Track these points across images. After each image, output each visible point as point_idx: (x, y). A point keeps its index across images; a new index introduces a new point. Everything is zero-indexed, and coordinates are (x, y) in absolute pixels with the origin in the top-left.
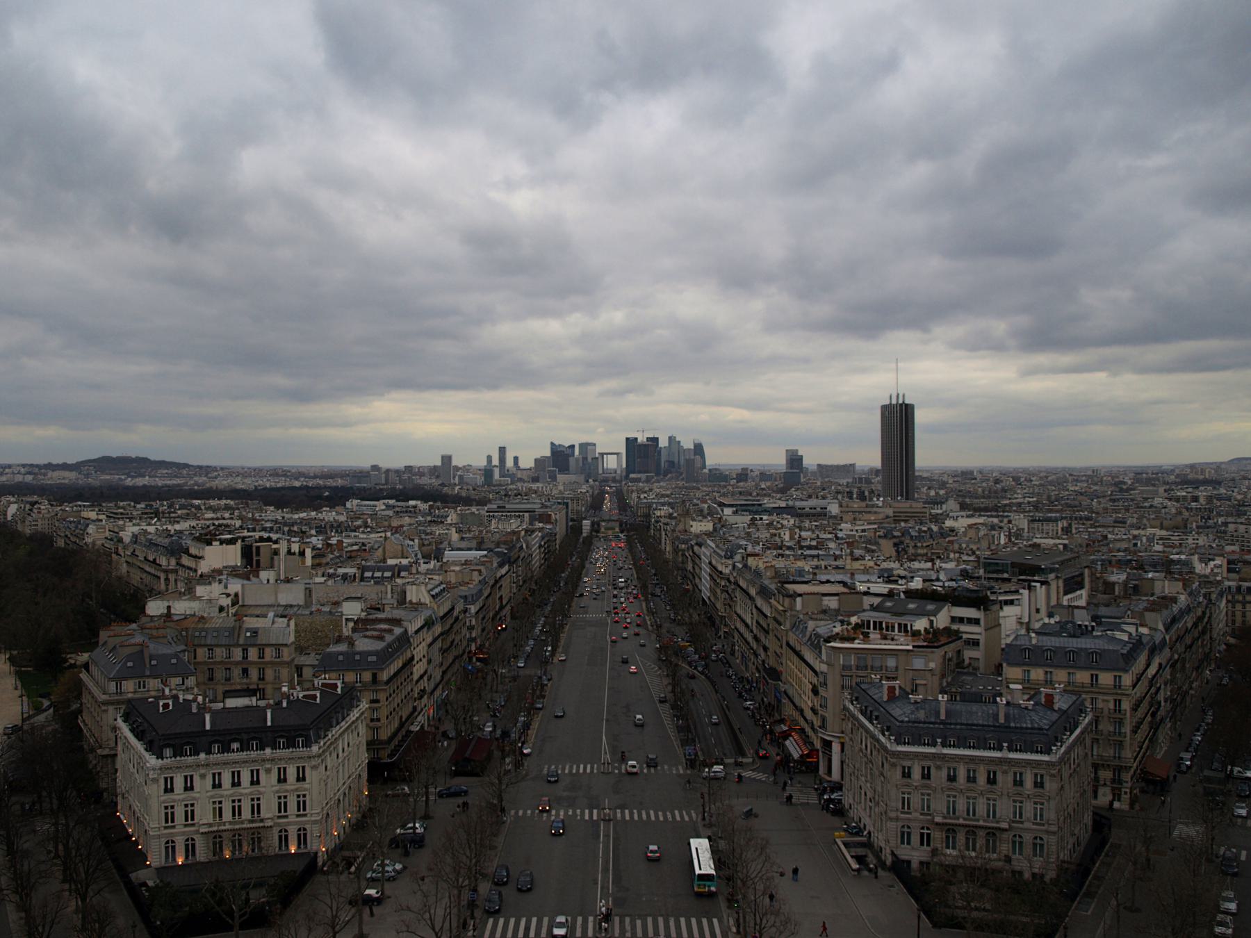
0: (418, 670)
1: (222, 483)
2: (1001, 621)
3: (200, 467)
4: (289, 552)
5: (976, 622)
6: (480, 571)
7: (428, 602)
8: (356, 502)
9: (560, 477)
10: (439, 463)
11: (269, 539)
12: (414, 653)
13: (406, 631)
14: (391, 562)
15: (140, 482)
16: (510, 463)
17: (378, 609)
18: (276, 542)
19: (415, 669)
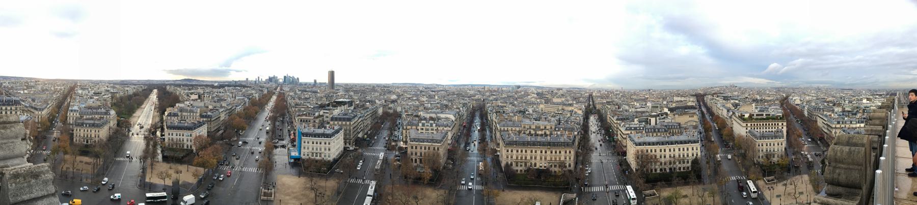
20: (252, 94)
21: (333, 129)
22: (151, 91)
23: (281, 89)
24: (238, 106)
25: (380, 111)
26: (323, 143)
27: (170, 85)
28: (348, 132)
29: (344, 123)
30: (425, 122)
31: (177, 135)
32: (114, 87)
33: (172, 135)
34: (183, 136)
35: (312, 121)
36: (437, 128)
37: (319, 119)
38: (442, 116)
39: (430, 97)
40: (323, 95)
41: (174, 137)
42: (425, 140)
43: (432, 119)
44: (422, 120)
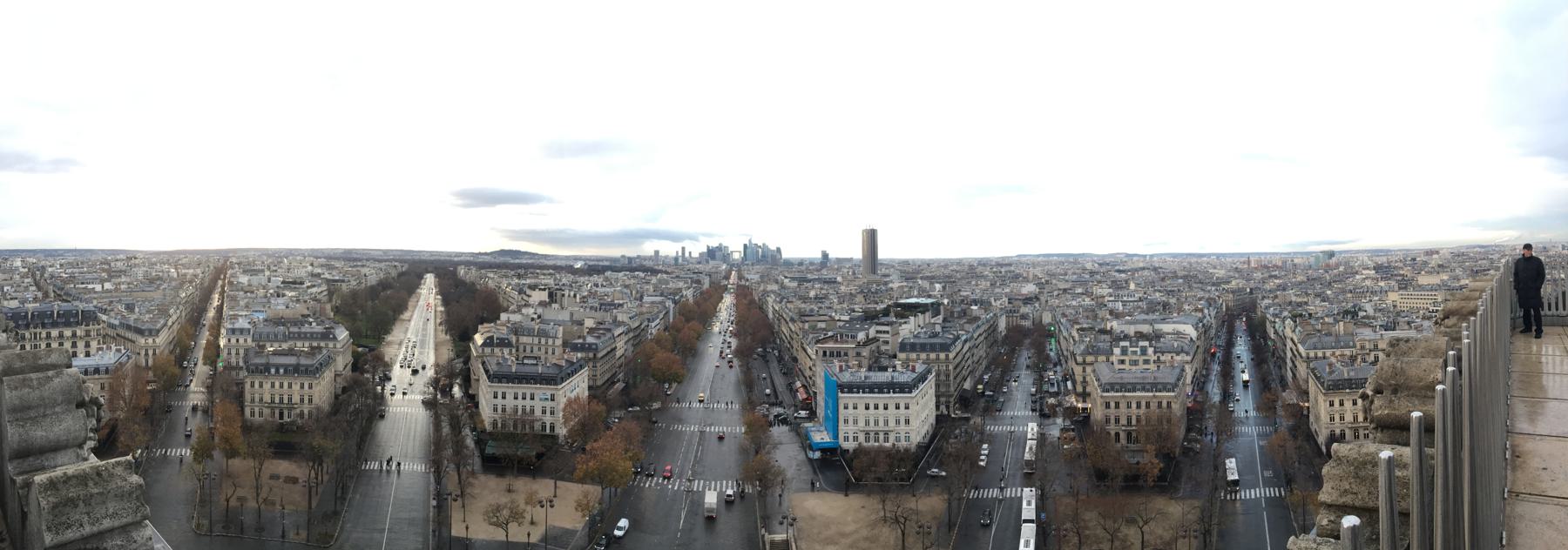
0: (619, 353)
4: (569, 296)
5: (888, 332)
11: (561, 289)
14: (616, 302)
20: (680, 290)
21: (913, 370)
22: (420, 277)
23: (740, 277)
24: (653, 321)
25: (1002, 324)
27: (468, 264)
29: (933, 356)
30: (1127, 344)
31: (516, 398)
32: (330, 267)
33: (504, 398)
34: (532, 399)
35: (852, 353)
36: (1158, 357)
37: (868, 348)
38: (1166, 328)
39: (1117, 285)
40: (853, 289)
41: (510, 402)
42: (1138, 387)
43: (1141, 336)
44: (1121, 340)
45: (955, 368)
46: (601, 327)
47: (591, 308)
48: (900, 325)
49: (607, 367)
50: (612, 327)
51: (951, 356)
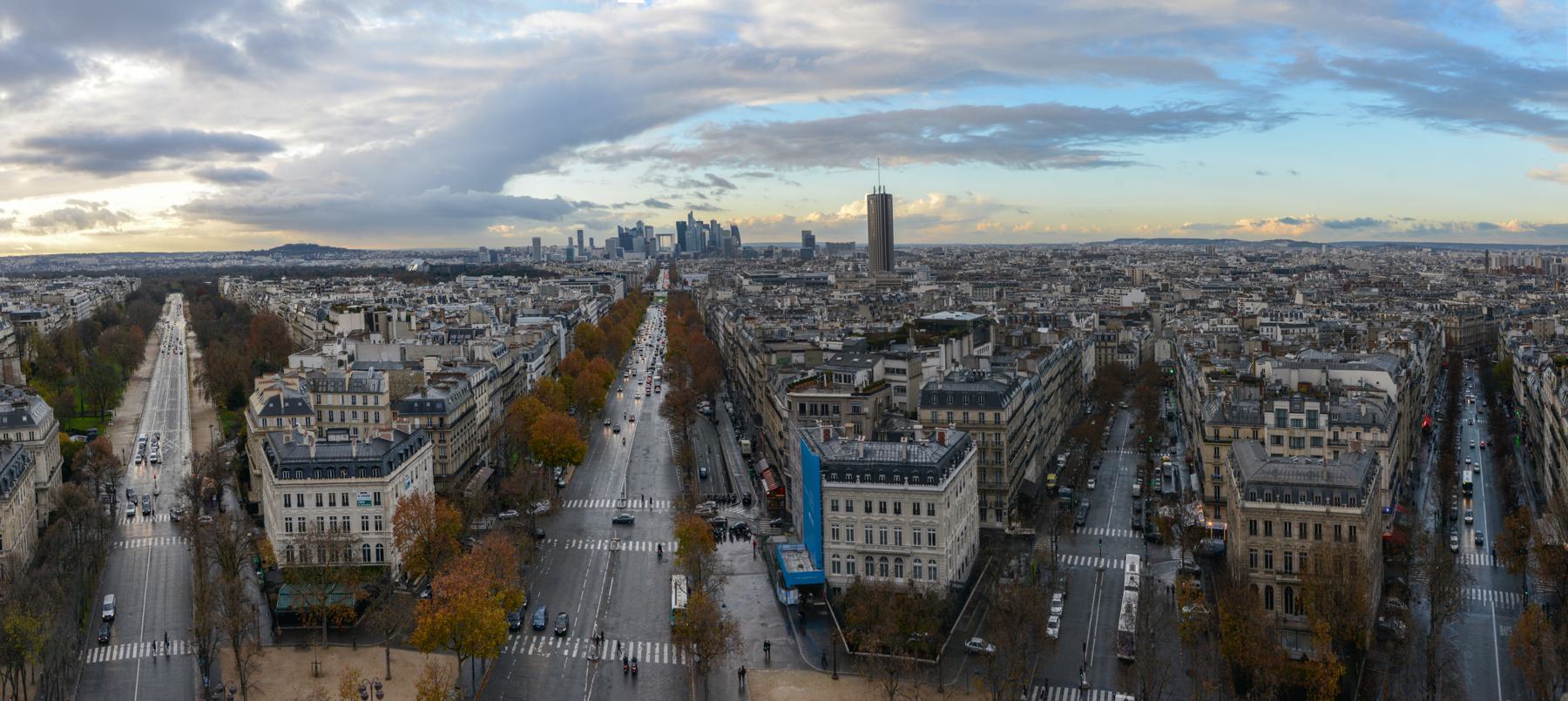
0: (480, 415)
1: (368, 264)
2: (924, 371)
3: (354, 251)
4: (399, 319)
5: (903, 372)
6: (540, 334)
7: (490, 359)
8: (463, 277)
9: (626, 255)
10: (531, 244)
11: (384, 309)
12: (477, 402)
13: (469, 383)
14: (474, 326)
15: (313, 263)
16: (586, 244)
17: (451, 365)
18: (389, 311)
19: (477, 416)
21: (941, 442)
22: (160, 300)
24: (534, 359)
25: (1089, 361)
26: (907, 509)
27: (234, 272)
28: (990, 457)
29: (973, 415)
35: (846, 409)
37: (872, 399)
38: (1349, 377)
43: (1308, 391)
44: (1276, 397)
45: (1011, 440)
46: (451, 371)
47: (435, 339)
48: (924, 360)
49: (462, 441)
50: (466, 370)
51: (1004, 416)
